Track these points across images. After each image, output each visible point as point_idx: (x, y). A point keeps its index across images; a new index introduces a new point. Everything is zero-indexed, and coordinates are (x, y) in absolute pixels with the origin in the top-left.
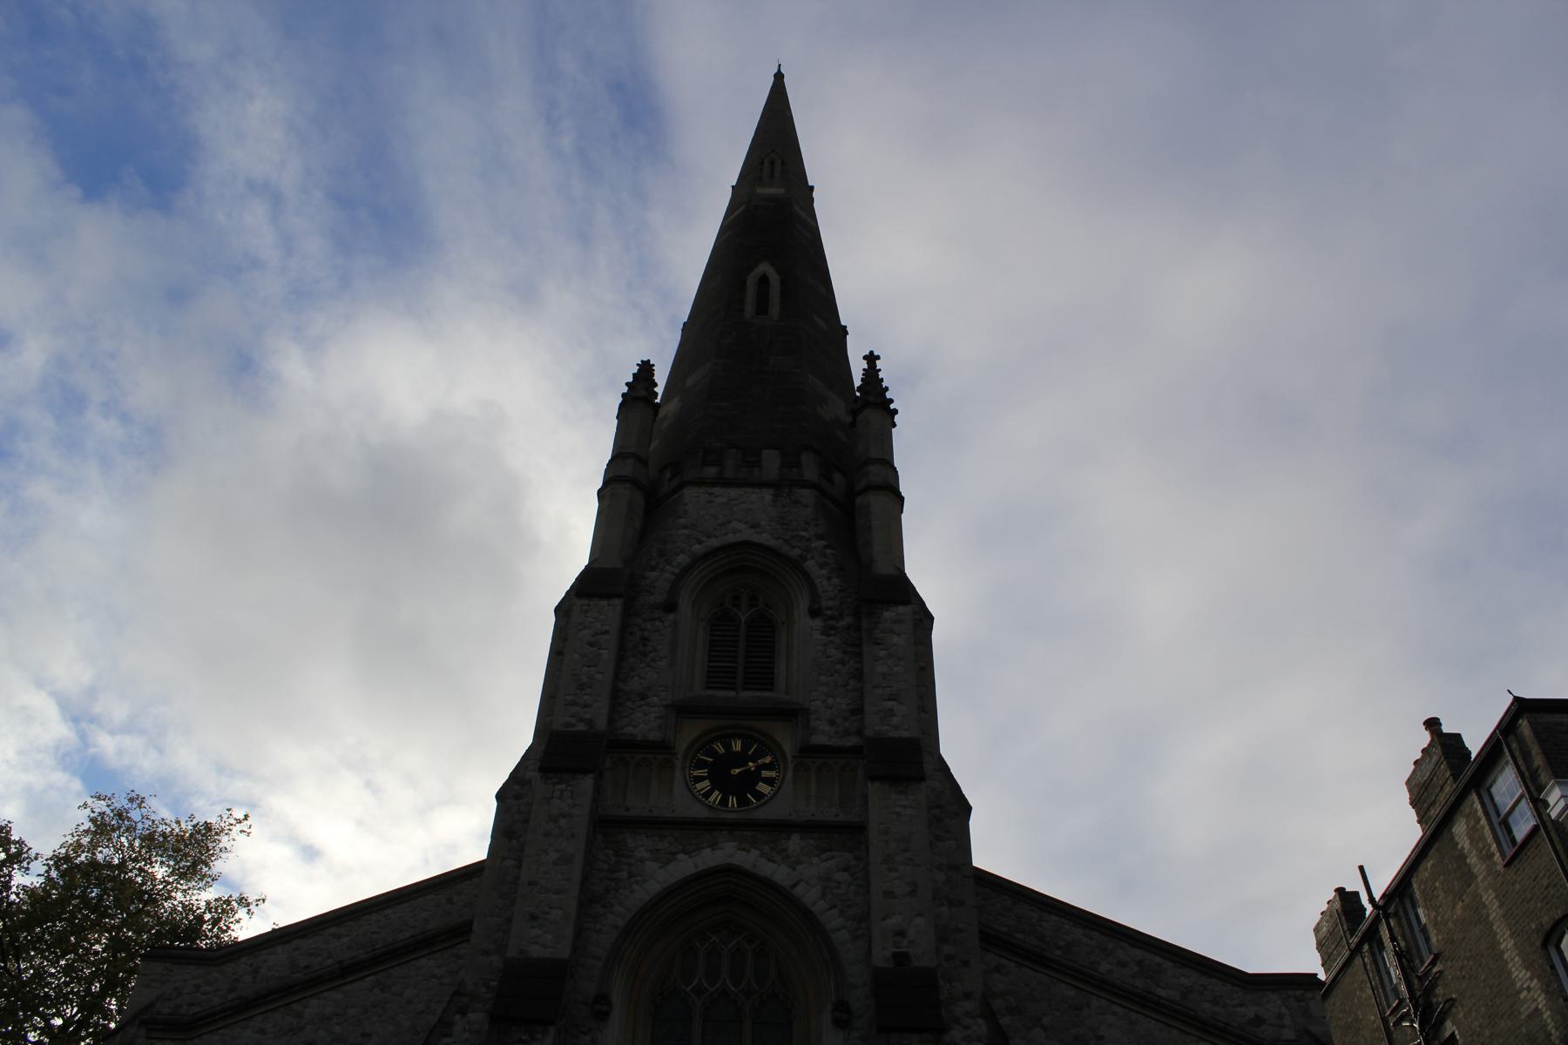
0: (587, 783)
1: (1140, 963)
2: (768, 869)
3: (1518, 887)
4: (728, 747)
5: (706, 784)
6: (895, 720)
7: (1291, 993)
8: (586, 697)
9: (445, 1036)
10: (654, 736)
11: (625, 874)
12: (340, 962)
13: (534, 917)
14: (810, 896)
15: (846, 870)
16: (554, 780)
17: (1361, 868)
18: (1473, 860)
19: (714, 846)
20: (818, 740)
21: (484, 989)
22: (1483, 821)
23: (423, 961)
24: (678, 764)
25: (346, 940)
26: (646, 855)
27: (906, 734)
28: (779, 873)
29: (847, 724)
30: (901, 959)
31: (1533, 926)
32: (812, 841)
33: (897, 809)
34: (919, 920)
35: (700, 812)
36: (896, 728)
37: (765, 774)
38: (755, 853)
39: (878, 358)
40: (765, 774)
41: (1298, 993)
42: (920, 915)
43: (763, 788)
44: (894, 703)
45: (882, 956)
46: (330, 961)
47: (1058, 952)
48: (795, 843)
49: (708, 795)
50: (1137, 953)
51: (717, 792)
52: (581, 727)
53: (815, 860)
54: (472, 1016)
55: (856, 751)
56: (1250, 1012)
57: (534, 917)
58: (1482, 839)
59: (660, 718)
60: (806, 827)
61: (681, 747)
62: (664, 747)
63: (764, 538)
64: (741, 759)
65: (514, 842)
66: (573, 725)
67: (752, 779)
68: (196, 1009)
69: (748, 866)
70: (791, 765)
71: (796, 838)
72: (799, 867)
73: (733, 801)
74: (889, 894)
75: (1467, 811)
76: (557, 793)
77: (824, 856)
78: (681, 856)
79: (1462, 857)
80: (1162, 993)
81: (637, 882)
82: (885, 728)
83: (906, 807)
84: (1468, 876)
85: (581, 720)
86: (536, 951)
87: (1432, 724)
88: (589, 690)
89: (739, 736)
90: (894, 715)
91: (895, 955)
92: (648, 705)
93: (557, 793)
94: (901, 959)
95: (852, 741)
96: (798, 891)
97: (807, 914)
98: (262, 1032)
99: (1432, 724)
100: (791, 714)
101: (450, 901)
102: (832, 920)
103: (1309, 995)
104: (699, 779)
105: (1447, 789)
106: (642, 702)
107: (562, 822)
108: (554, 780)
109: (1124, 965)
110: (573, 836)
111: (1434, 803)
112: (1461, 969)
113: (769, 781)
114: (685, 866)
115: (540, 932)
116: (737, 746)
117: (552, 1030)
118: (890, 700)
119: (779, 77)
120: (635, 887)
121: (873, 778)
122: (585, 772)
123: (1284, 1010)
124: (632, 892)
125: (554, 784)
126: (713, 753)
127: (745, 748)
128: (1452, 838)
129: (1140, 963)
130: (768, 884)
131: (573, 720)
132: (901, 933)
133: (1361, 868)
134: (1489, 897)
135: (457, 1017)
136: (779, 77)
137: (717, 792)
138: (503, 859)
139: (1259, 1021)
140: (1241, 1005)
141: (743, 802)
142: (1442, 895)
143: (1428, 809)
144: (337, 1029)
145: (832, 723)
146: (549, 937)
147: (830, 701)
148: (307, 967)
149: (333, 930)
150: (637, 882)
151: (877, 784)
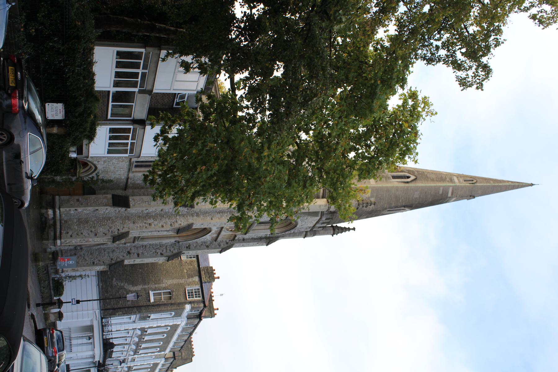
3: (181, 289)
39: (355, 230)
48: (215, 235)
55: (234, 239)
63: (298, 226)
79: (192, 277)
87: (218, 278)
95: (236, 238)
97: (199, 238)
99: (218, 278)
100: (246, 234)
105: (205, 279)
111: (204, 274)
112: (176, 266)
119: (532, 185)
134: (182, 281)
136: (532, 185)
143: (205, 271)
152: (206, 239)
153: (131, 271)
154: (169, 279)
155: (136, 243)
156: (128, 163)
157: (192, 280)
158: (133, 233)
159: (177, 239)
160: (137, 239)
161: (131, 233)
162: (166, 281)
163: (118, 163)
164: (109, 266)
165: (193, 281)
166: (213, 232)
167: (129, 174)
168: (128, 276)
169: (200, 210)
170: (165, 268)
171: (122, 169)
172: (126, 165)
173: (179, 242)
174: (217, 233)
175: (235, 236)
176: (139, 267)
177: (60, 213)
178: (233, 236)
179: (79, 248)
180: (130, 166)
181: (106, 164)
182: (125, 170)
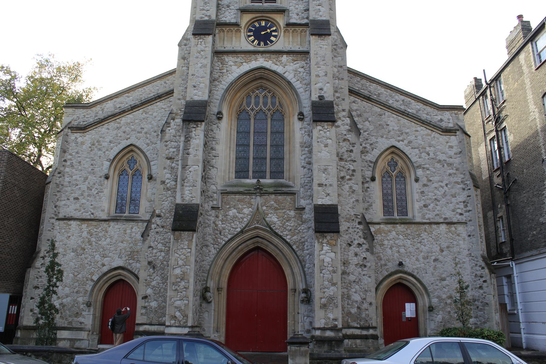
0: (210, 38)
1: (403, 101)
2: (274, 68)
3: (538, 77)
4: (260, 24)
5: (253, 37)
6: (321, 14)
7: (453, 112)
8: (207, 7)
9: (168, 127)
10: (233, 21)
11: (225, 71)
12: (131, 105)
13: (195, 87)
14: (289, 76)
15: (302, 68)
16: (198, 38)
17: (484, 70)
18: (524, 68)
19: (256, 60)
20: (293, 21)
21: (180, 111)
22: (531, 54)
23: (158, 103)
24: (242, 31)
25: (131, 98)
26: (232, 64)
27: (324, 19)
28: (279, 69)
29: (303, 15)
30: (321, 98)
31: (540, 91)
32: (290, 58)
33: (321, 46)
34: (328, 85)
35: (251, 48)
36: (321, 16)
37: (273, 34)
38: (270, 62)
40: (273, 34)
41: (456, 112)
42: (328, 83)
43: (272, 38)
44: (320, 7)
45: (315, 98)
46: (127, 105)
47: (375, 96)
48: (284, 58)
49: (253, 42)
50: (402, 97)
51: (256, 41)
52: (206, 18)
53: (292, 64)
54: (176, 120)
55: (306, 25)
56: (439, 118)
57: (195, 87)
58: (530, 60)
59: (235, 14)
60: (289, 53)
61: (243, 25)
62: (236, 25)
64: (265, 28)
65: (186, 61)
66: (204, 18)
67: (269, 35)
68: (86, 123)
69: (268, 67)
70: (283, 31)
71: (285, 56)
72: (286, 67)
73: (262, 43)
74: (318, 76)
75: (526, 50)
76: (199, 43)
77: (295, 63)
78: (244, 64)
79: (521, 67)
80: (409, 110)
81: (230, 73)
82: (317, 16)
83: (324, 45)
84: (521, 73)
85: (206, 16)
86: (196, 98)
88: (208, 4)
89: (264, 20)
90: (320, 12)
91: (319, 96)
92: (230, 9)
93: (199, 43)
94: (321, 98)
95: (305, 21)
96: (285, 75)
97: (289, 83)
98: (108, 129)
100: (282, 11)
101: (165, 83)
102: (297, 85)
103: (459, 113)
104: (249, 36)
106: (228, 8)
107: (202, 53)
108: (198, 38)
109: (397, 101)
110: (206, 58)
113: (275, 36)
114: (246, 67)
115: (197, 91)
116: (263, 24)
117: (203, 123)
118: (319, 5)
120: (229, 75)
121: (312, 35)
122: (209, 34)
123: (450, 117)
124: (228, 76)
125: (198, 39)
126: (254, 27)
127: (266, 24)
128: (519, 60)
129: (403, 101)
130: (275, 72)
131: (203, 16)
132: (321, 89)
133: (484, 70)
134: (527, 81)
135: (172, 121)
137: (256, 41)
138: (182, 67)
139: (441, 120)
140: (436, 115)
141: (266, 44)
142: (511, 80)
144: (133, 127)
145: (298, 15)
146: (200, 93)
147: (297, 6)
148: (119, 107)
149: (127, 94)
150: (230, 73)
151: (314, 37)
152: (302, 70)
153: (528, 190)
154: (529, 110)
155: (297, 187)
156: (112, 224)
157: (524, 65)
158: (187, 198)
159: (296, 117)
160: (284, 189)
161: (183, 200)
162: (531, 114)
163: (111, 237)
164: (318, 234)
165: (525, 61)
166: (269, 64)
167: (141, 220)
168: (535, 193)
169: (179, 99)
170: (517, 126)
171: (128, 231)
172: (117, 226)
173: (301, 114)
174: (273, 56)
175: (288, 25)
176: (522, 176)
177: (151, 324)
178: (291, 29)
179: (303, 295)
180: (118, 220)
181: (110, 254)
182: (130, 226)
